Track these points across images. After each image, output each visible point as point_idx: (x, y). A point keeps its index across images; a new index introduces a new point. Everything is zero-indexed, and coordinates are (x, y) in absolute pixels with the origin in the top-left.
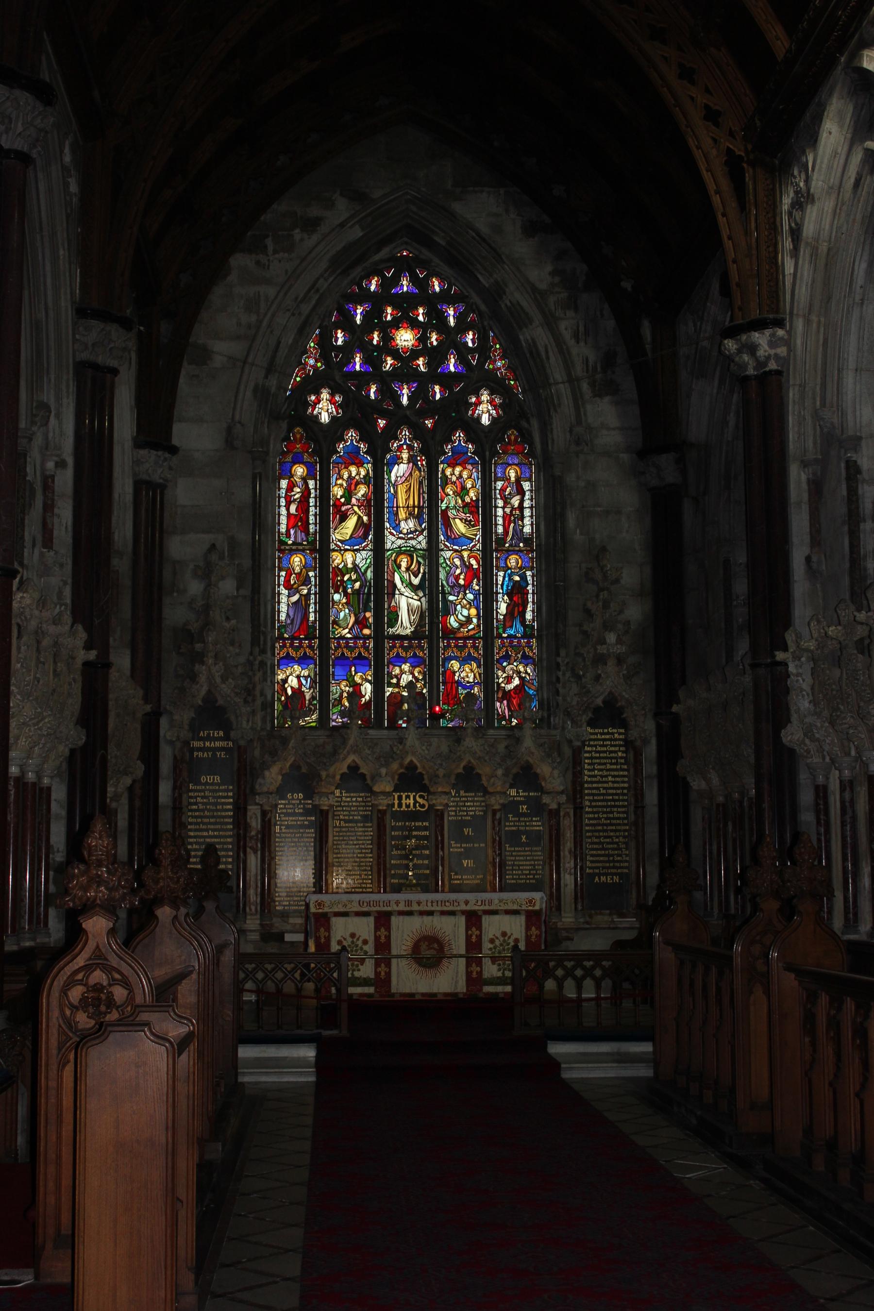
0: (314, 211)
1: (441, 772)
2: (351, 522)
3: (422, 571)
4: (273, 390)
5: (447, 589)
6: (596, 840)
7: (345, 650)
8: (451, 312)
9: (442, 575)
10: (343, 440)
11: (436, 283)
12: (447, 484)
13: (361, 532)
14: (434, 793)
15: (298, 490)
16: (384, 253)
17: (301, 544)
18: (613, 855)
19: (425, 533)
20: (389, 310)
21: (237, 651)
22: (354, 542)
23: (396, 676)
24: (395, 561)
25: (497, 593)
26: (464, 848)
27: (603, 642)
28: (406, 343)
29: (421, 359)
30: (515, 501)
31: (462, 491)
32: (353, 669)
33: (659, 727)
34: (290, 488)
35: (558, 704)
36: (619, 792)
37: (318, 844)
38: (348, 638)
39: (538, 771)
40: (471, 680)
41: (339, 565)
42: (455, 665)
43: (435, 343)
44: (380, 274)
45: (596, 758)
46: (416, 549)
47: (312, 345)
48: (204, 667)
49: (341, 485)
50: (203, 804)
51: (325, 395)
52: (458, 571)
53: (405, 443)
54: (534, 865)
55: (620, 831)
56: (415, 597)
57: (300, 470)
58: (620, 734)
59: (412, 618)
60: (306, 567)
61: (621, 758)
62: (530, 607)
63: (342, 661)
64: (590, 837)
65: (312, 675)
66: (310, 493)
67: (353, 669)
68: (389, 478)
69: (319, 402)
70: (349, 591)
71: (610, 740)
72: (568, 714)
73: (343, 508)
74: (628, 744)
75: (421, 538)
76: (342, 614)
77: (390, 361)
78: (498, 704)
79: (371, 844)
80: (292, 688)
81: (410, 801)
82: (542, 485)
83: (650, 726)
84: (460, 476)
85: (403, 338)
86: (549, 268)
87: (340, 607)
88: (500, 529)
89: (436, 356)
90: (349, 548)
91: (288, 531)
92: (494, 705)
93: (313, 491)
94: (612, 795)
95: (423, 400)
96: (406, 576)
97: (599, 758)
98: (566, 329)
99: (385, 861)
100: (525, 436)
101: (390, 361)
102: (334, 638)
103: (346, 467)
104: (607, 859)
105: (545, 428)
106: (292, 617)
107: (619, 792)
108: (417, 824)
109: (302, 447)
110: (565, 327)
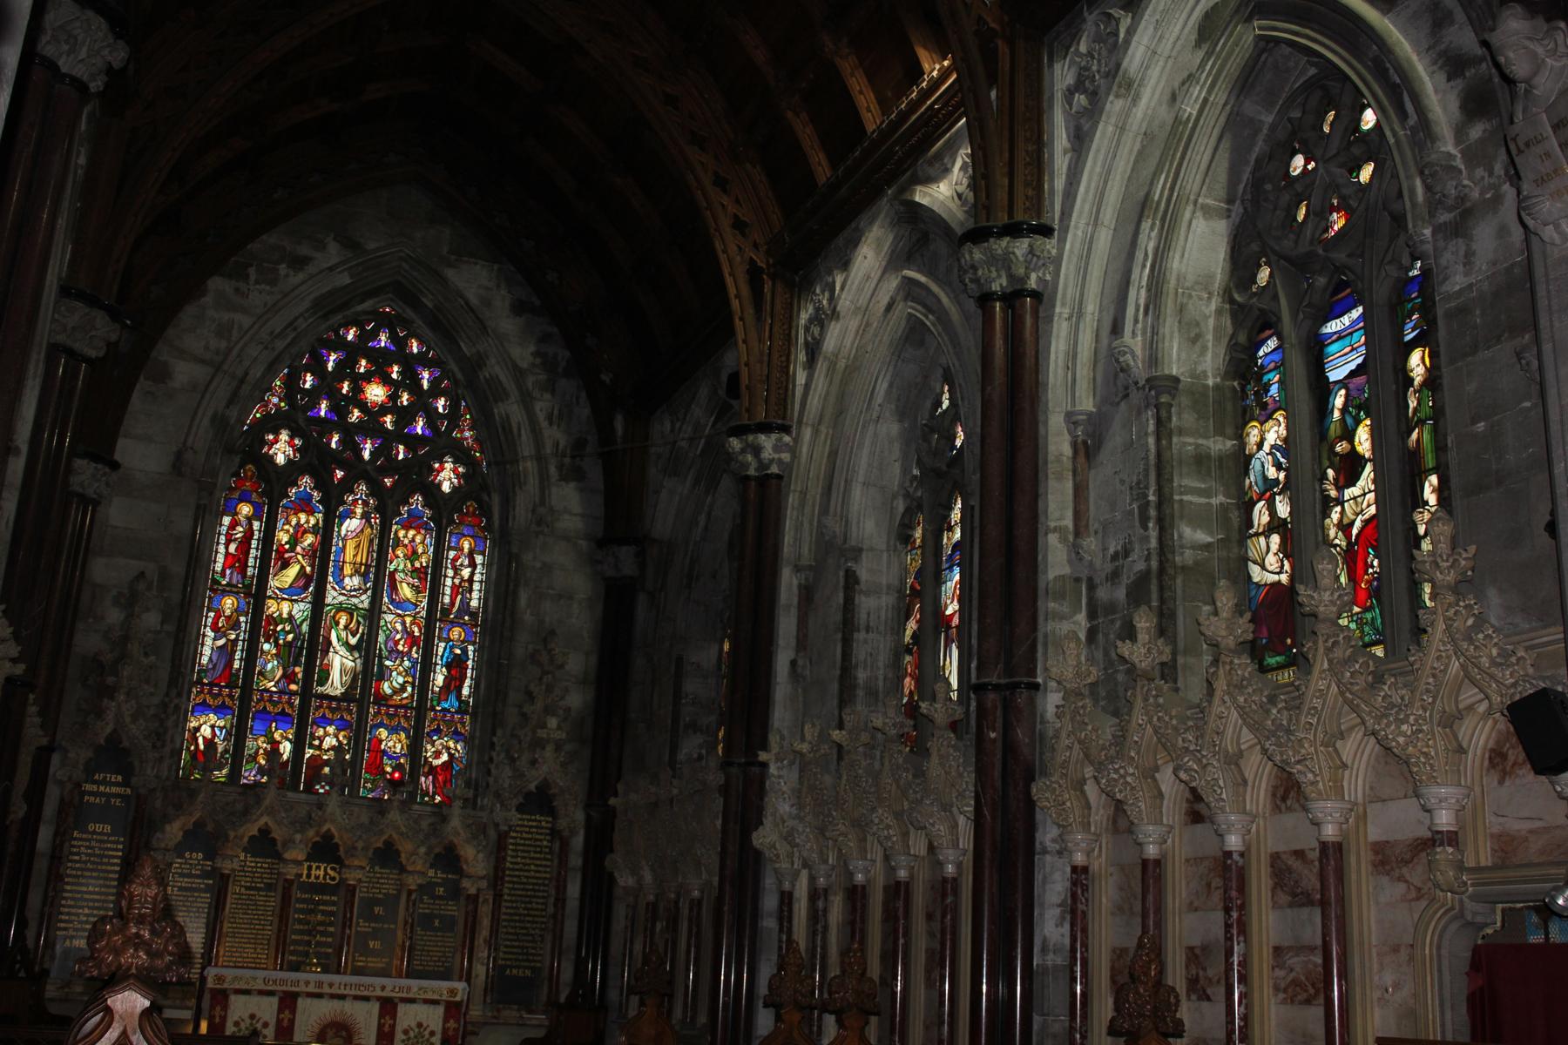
0: (304, 250)
1: (360, 845)
2: (293, 571)
3: (360, 631)
4: (232, 421)
5: (385, 653)
6: (513, 931)
7: (267, 704)
8: (426, 375)
9: (381, 638)
10: (297, 485)
11: (415, 344)
12: (398, 546)
13: (302, 582)
14: (349, 867)
15: (241, 529)
16: (367, 305)
17: (236, 586)
18: (527, 948)
19: (369, 593)
20: (363, 362)
21: (152, 690)
22: (292, 592)
23: (319, 738)
24: (334, 617)
25: (436, 664)
26: (373, 928)
27: (544, 726)
28: (376, 398)
29: (389, 416)
30: (466, 573)
31: (413, 555)
32: (274, 725)
33: (588, 818)
34: (233, 526)
35: (488, 785)
36: (540, 881)
37: (213, 911)
38: (272, 692)
39: (462, 853)
40: (398, 751)
41: (274, 613)
42: (383, 733)
43: (405, 403)
44: (360, 325)
45: (520, 845)
46: (357, 608)
47: (278, 383)
48: (114, 704)
49: (288, 531)
50: (87, 854)
51: (284, 436)
52: (398, 637)
53: (361, 498)
54: (444, 952)
55: (537, 922)
56: (350, 658)
57: (246, 509)
58: (547, 822)
59: (344, 678)
60: (238, 611)
61: (546, 847)
62: (468, 682)
63: (263, 715)
64: (505, 927)
65: (228, 726)
66: (253, 534)
67: (274, 725)
68: (339, 532)
69: (277, 442)
70: (281, 642)
71: (536, 827)
72: (497, 795)
73: (287, 555)
74: (554, 833)
75: (364, 597)
76: (270, 666)
77: (356, 413)
78: (423, 779)
79: (272, 916)
80: (204, 737)
81: (320, 872)
82: (496, 560)
83: (580, 816)
84: (413, 540)
85: (374, 393)
86: (532, 348)
87: (269, 657)
88: (447, 600)
89: (405, 416)
90: (286, 597)
91: (223, 571)
92: (419, 779)
93: (256, 533)
94: (534, 884)
95: (386, 459)
96: (343, 634)
97: (524, 845)
98: (541, 410)
99: (285, 937)
100: (485, 510)
101: (356, 413)
102: (258, 690)
103: (296, 514)
104: (520, 951)
105: (507, 503)
106: (215, 661)
107: (540, 881)
108: (325, 898)
109: (251, 486)
110: (541, 407)
